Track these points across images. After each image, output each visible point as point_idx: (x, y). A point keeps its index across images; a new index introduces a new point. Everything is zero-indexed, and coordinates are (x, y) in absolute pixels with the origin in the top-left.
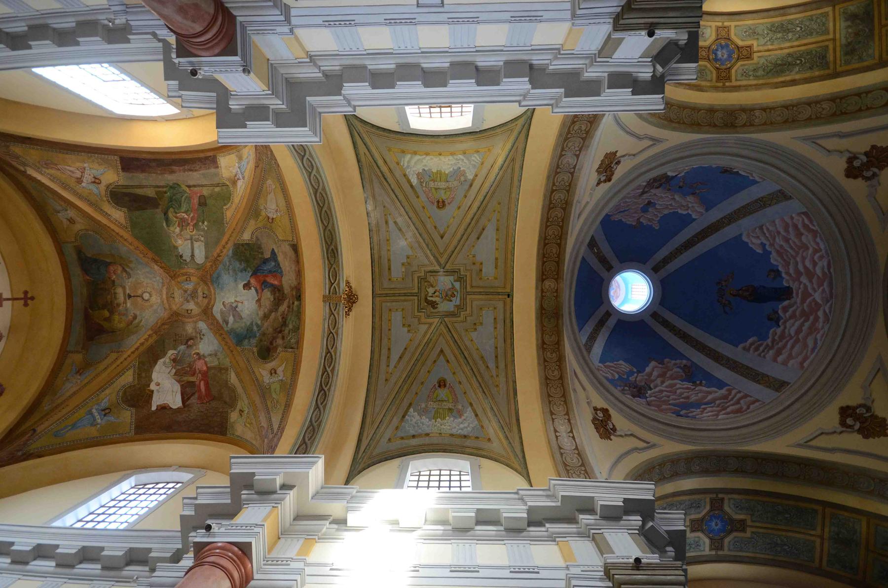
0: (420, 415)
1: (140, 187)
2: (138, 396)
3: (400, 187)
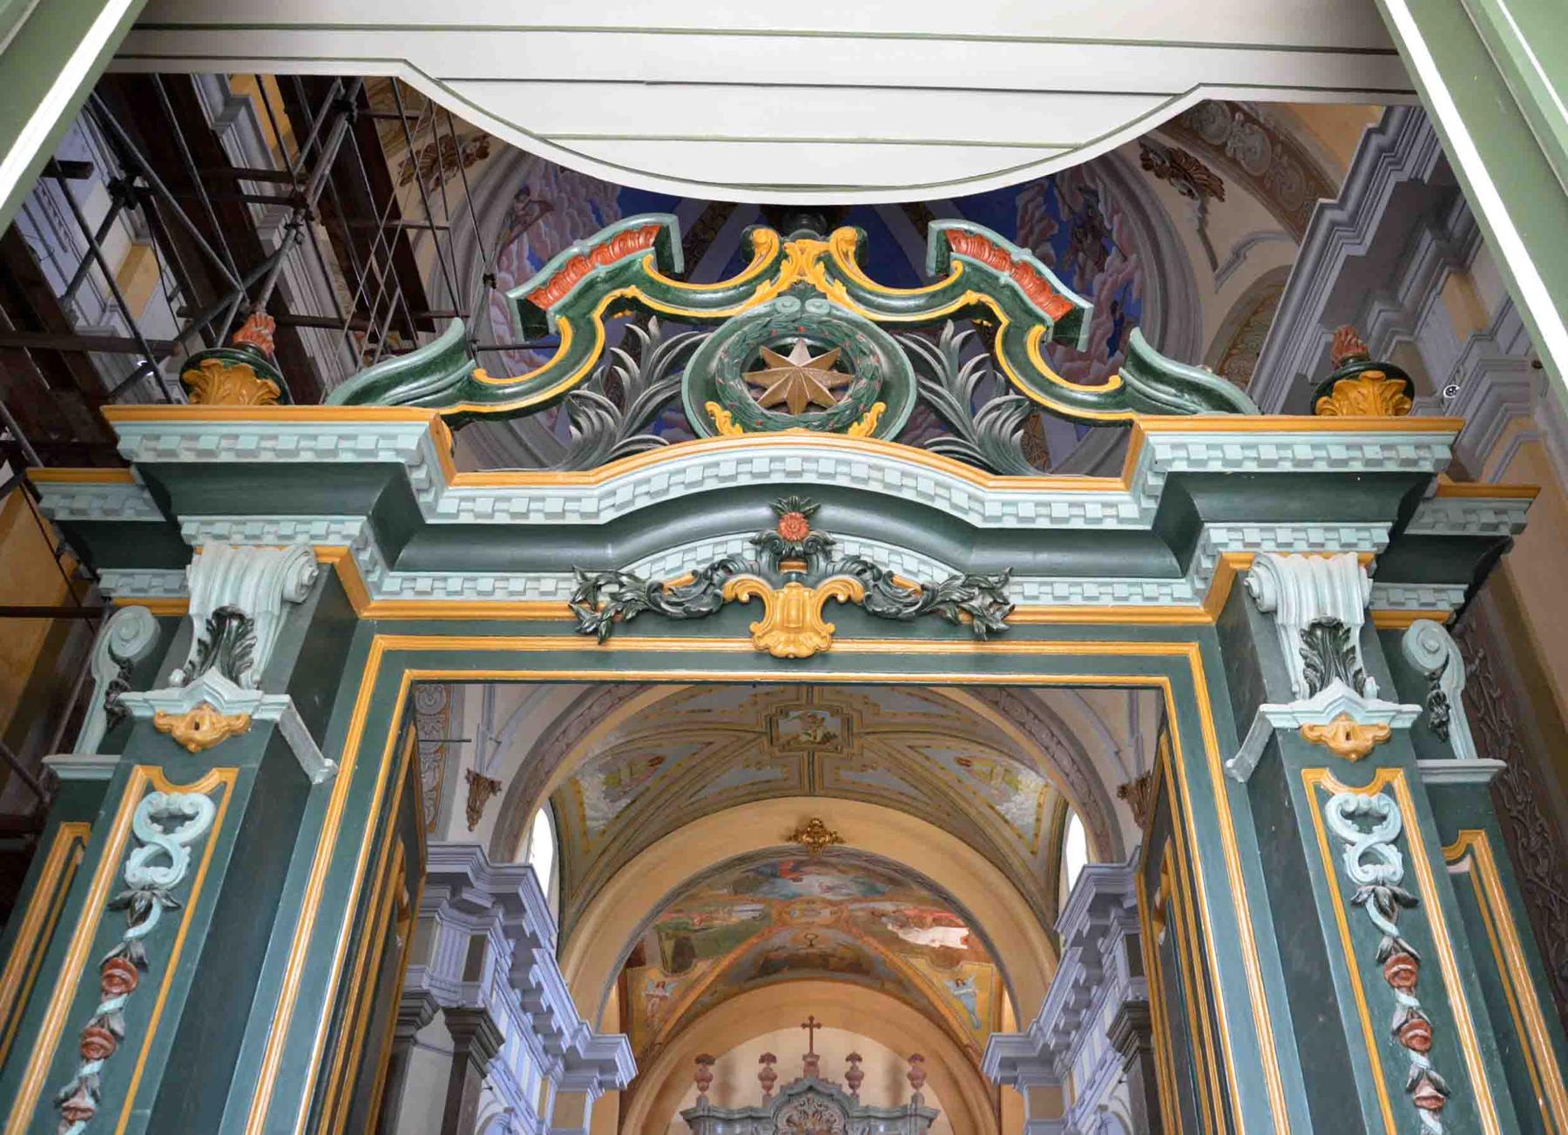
0: (1009, 801)
1: (663, 953)
2: (947, 958)
3: (635, 819)
